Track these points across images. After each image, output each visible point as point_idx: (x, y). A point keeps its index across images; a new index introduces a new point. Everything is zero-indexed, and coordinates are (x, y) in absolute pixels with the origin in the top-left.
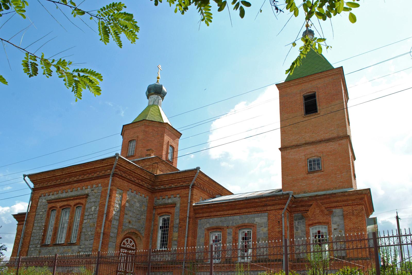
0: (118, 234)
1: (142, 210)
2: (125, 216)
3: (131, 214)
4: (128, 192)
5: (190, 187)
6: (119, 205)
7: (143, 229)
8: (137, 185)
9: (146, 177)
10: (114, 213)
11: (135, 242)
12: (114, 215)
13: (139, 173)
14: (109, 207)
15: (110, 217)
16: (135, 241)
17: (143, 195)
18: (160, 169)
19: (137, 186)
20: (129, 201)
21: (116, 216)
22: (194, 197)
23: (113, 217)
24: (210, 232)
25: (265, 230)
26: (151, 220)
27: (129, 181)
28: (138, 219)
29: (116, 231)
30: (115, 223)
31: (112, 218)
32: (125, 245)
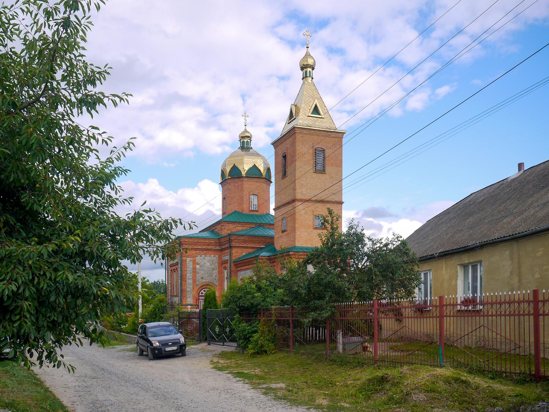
0: (193, 288)
2: (197, 275)
3: (202, 272)
17: (213, 256)
26: (220, 273)
27: (196, 249)
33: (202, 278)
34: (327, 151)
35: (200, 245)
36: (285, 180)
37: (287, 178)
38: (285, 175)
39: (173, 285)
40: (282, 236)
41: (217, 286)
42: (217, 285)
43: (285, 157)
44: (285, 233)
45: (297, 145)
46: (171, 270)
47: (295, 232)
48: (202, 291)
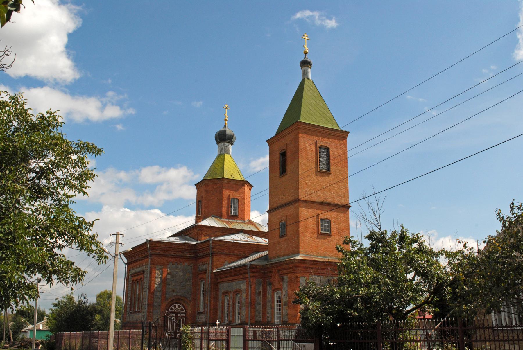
1: (187, 277)
2: (168, 286)
3: (174, 284)
4: (169, 266)
5: (210, 256)
6: (160, 279)
7: (189, 294)
8: (177, 257)
9: (185, 248)
10: (156, 286)
11: (183, 306)
12: (156, 288)
13: (176, 247)
14: (150, 281)
15: (152, 290)
16: (184, 304)
17: (187, 264)
18: (205, 234)
19: (178, 258)
20: (171, 273)
21: (159, 288)
22: (215, 264)
23: (155, 290)
24: (225, 296)
25: (245, 295)
28: (183, 286)
29: (160, 300)
30: (158, 294)
31: (154, 290)
32: (173, 310)
33: (173, 291)
34: (331, 149)
35: (173, 251)
36: (284, 178)
37: (287, 177)
38: (283, 171)
39: (135, 298)
40: (279, 243)
41: (190, 301)
42: (191, 299)
43: (283, 155)
44: (283, 238)
45: (300, 140)
46: (133, 281)
47: (298, 237)
48: (172, 307)
